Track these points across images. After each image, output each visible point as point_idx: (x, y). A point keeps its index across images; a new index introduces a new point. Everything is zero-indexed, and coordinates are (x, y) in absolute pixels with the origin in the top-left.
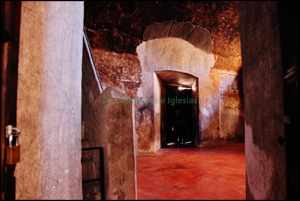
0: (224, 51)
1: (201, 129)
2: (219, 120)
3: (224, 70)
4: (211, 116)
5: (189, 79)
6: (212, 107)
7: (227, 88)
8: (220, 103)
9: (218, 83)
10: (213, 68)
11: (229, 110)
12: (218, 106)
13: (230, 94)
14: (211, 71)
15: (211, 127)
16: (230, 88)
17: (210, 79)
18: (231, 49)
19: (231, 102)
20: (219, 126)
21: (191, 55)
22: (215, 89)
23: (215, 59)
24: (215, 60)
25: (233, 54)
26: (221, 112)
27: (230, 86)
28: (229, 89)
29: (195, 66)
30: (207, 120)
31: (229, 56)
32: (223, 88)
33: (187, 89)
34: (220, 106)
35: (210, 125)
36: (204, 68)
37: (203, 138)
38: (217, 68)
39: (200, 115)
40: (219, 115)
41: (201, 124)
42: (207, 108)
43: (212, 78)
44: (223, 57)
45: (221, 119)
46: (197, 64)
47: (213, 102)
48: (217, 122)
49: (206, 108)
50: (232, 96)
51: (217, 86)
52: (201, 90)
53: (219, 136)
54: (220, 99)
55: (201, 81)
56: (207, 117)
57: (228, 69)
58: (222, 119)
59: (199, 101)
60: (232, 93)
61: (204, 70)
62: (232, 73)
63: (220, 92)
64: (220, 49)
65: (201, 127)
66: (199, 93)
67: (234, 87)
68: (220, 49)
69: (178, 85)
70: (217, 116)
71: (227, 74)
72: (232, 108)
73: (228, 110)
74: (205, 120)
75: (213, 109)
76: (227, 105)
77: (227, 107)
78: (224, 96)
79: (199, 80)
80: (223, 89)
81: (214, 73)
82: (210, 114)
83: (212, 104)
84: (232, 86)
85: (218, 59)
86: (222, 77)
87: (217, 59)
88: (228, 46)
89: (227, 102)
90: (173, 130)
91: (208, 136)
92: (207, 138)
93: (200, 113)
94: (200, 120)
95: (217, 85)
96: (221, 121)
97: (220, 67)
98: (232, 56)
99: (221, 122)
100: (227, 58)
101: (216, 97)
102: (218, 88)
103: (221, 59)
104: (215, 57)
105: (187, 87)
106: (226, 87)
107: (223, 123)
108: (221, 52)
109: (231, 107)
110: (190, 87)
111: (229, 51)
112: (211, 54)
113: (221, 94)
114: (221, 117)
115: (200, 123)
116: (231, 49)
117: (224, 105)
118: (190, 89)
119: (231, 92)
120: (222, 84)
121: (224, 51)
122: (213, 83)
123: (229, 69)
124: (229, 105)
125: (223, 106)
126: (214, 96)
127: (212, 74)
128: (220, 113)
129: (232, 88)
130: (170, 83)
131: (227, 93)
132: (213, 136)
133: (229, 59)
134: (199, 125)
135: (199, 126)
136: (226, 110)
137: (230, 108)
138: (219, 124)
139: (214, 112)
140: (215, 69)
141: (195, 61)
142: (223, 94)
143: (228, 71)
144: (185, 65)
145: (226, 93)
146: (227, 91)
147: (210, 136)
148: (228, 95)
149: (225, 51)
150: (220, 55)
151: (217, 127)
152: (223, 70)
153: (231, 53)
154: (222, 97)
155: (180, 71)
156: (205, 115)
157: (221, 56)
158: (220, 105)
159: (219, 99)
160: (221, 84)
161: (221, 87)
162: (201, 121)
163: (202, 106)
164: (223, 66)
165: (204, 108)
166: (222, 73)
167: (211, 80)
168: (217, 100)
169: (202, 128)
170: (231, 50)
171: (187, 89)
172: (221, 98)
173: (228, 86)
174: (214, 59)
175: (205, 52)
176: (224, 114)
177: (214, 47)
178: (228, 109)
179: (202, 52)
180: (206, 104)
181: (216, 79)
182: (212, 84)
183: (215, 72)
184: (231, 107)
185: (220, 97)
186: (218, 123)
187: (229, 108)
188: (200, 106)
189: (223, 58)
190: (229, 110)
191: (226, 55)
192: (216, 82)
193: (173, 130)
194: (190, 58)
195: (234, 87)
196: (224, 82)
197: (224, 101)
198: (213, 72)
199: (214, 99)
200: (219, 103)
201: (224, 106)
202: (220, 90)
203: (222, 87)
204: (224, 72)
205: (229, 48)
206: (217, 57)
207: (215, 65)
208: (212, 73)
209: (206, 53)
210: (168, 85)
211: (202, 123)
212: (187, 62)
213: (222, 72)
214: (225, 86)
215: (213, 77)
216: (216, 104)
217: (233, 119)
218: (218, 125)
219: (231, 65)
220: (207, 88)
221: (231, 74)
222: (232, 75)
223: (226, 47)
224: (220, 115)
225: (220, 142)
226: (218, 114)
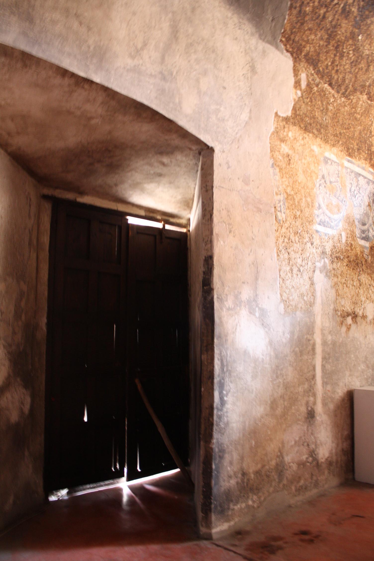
0: (337, 58)
1: (221, 432)
2: (314, 377)
3: (335, 150)
4: (277, 357)
5: (165, 160)
6: (282, 306)
7: (345, 230)
8: (318, 294)
9: (309, 199)
10: (286, 119)
11: (353, 327)
12: (312, 304)
13: (356, 255)
14: (276, 132)
15: (279, 411)
16: (358, 233)
17: (271, 170)
18: (363, 58)
19: (361, 292)
20: (315, 403)
21: (173, 13)
22: (298, 223)
23: (297, 84)
24: (295, 87)
25: (369, 86)
26: (323, 334)
27: (357, 223)
28: (352, 235)
29: (198, 81)
30: (254, 377)
31: (355, 90)
32: (331, 227)
33: (168, 227)
34: (318, 308)
35: (273, 404)
36: (247, 110)
37: (233, 482)
38: (306, 129)
39: (216, 351)
40: (313, 349)
41: (223, 402)
42: (257, 314)
43: (281, 169)
44: (330, 85)
45: (323, 366)
46: (205, 73)
47: (288, 282)
48: (306, 386)
49: (252, 312)
50: (364, 267)
51: (307, 212)
52: (224, 213)
53: (312, 453)
54: (317, 272)
55: (229, 167)
56: (256, 360)
57: (348, 149)
58: (328, 367)
59: (216, 271)
60: (362, 252)
61: (245, 116)
62: (364, 169)
63: (317, 241)
64: (321, 39)
65: (220, 417)
66: (216, 230)
67: (368, 230)
68: (321, 39)
69: (121, 208)
70: (305, 357)
71: (344, 170)
72: (364, 317)
73: (349, 329)
74: (248, 378)
75: (288, 320)
76: (348, 308)
77: (348, 315)
78: (332, 262)
79: (218, 158)
80: (330, 232)
81: (293, 148)
82: (271, 343)
83: (285, 296)
84: (364, 224)
85: (308, 85)
86: (323, 177)
87: (304, 84)
88: (353, 36)
89: (346, 290)
90: (86, 419)
91: (259, 466)
92: (257, 473)
93: (220, 337)
94: (216, 380)
95: (303, 204)
96: (323, 378)
97: (319, 131)
98: (365, 97)
99: (325, 383)
100: (346, 97)
101: (299, 261)
102: (311, 222)
103: (322, 94)
104: (296, 72)
105: (167, 222)
106: (341, 226)
107: (329, 387)
108: (322, 57)
109: (361, 313)
110: (183, 221)
111: (354, 63)
112: (277, 47)
113: (324, 253)
114: (324, 358)
115: (216, 394)
116: (363, 58)
117: (335, 302)
118: (184, 230)
119: (358, 250)
120: (323, 206)
121: (337, 58)
122: (288, 195)
123: (353, 149)
124: (355, 303)
125: (332, 307)
126: (293, 255)
127: (285, 148)
128: (318, 339)
129: (363, 232)
130: (82, 193)
131: (347, 251)
132: (288, 459)
133: (354, 107)
134: (211, 408)
135: (211, 414)
136: (344, 329)
137: (359, 319)
138: (314, 395)
139: (292, 333)
140: (297, 128)
141: (194, 57)
142: (332, 253)
143: (350, 155)
144: (133, 57)
145: (341, 251)
146: (344, 240)
147: (273, 463)
148: (350, 261)
149: (342, 56)
150: (318, 72)
151: (303, 409)
152: (328, 147)
153: (362, 77)
154: (325, 266)
155: (97, 79)
156: (246, 353)
157: (322, 75)
158: (319, 301)
159: (314, 271)
160: (319, 207)
161: (322, 217)
162: (222, 386)
163: (229, 303)
164: (331, 130)
165: (244, 312)
166: (326, 160)
167: (278, 177)
168: (306, 276)
169: (227, 424)
170: (363, 65)
171: (168, 227)
172: (321, 272)
173: (350, 221)
174: (292, 81)
175: (248, 27)
176: (334, 343)
177: (295, 12)
178: (349, 320)
179: (235, 19)
180: (256, 289)
181: (301, 178)
182: (281, 197)
183: (297, 146)
184: (361, 313)
185: (319, 265)
186: (311, 391)
187: (355, 316)
188: (220, 300)
189: (329, 88)
190: (353, 327)
191: (344, 80)
192: (303, 191)
193: (86, 419)
194: (166, 25)
195: (371, 230)
196: (334, 201)
197: (336, 284)
198: (289, 142)
199: (292, 270)
200: (313, 295)
201: (336, 310)
202: (317, 231)
203: (327, 220)
204: (333, 157)
205: (356, 50)
206: (303, 76)
207: (294, 109)
208: (283, 145)
209: (257, 36)
210: (70, 196)
211: (229, 399)
212: (145, 44)
213: (327, 154)
214: (336, 217)
215: (289, 164)
216: (302, 295)
217: (368, 367)
218: (312, 399)
219: (360, 133)
220: (260, 210)
221: (360, 175)
222: (365, 178)
223: (347, 39)
224: (319, 349)
225: (316, 484)
226: (310, 348)
